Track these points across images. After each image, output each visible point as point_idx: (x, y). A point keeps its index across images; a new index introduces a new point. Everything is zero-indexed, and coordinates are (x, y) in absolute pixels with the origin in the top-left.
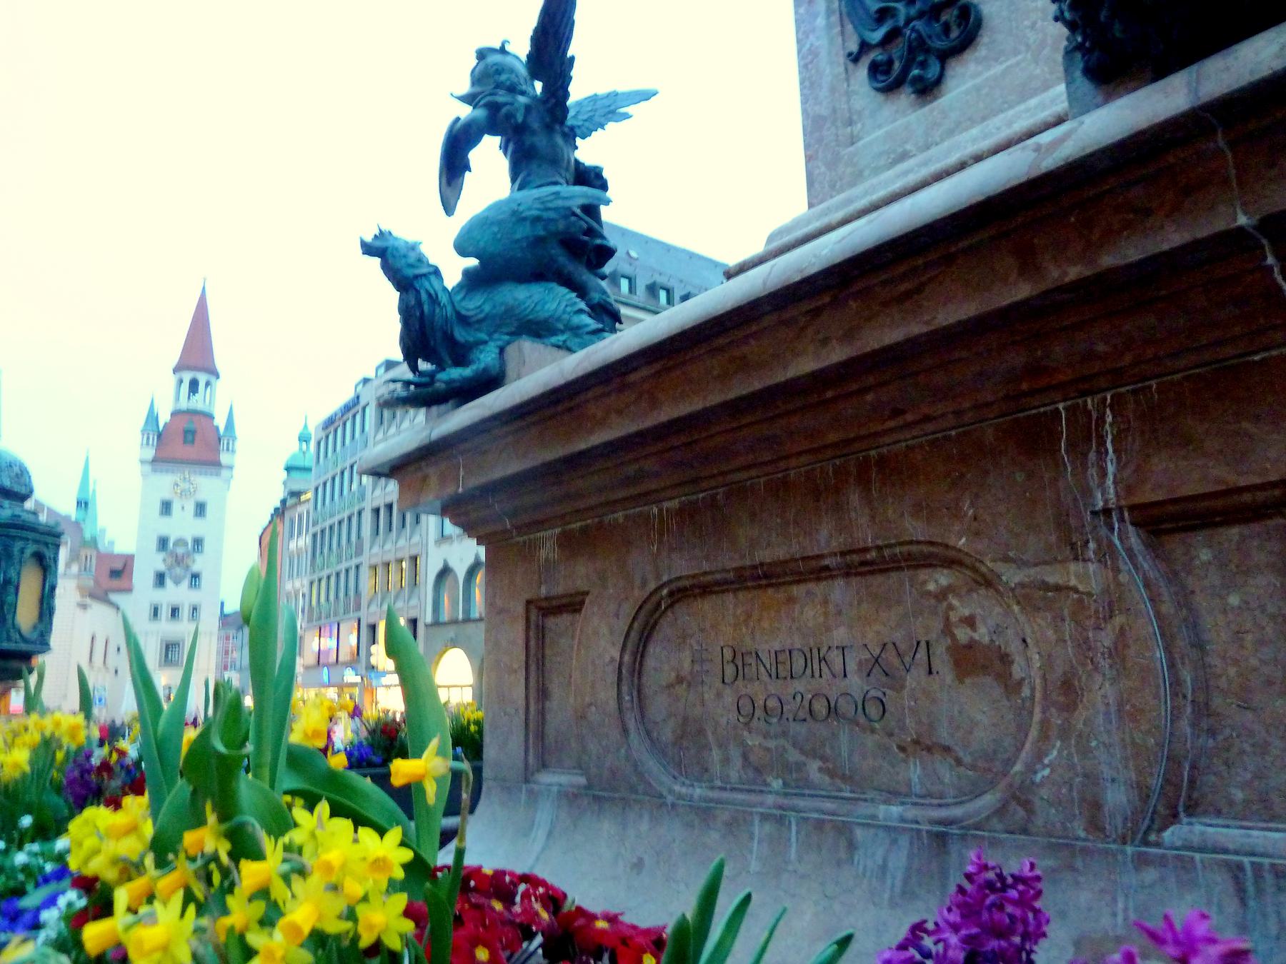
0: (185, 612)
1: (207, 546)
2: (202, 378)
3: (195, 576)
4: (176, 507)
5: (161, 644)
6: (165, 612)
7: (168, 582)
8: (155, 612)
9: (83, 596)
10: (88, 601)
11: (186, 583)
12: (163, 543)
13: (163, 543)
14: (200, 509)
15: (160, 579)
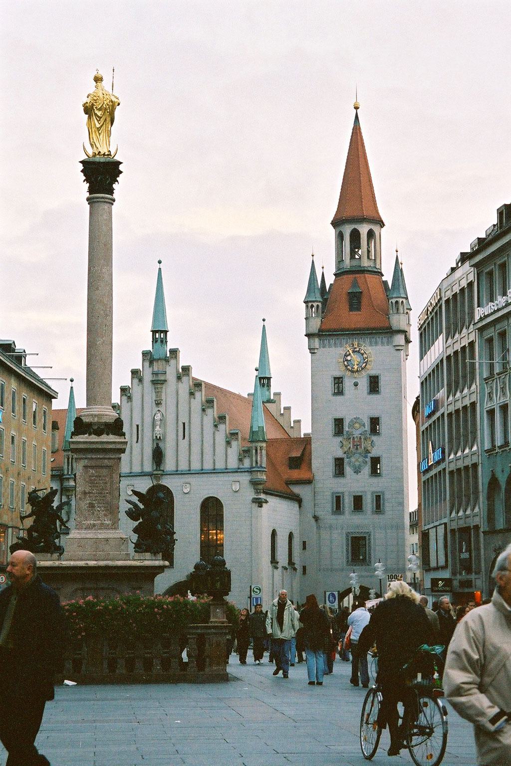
0: (368, 503)
1: (383, 427)
2: (364, 229)
3: (376, 461)
4: (348, 384)
5: (347, 539)
6: (348, 503)
7: (348, 470)
8: (338, 501)
9: (257, 492)
10: (263, 496)
11: (367, 470)
12: (339, 423)
13: (339, 423)
14: (374, 385)
15: (339, 466)
